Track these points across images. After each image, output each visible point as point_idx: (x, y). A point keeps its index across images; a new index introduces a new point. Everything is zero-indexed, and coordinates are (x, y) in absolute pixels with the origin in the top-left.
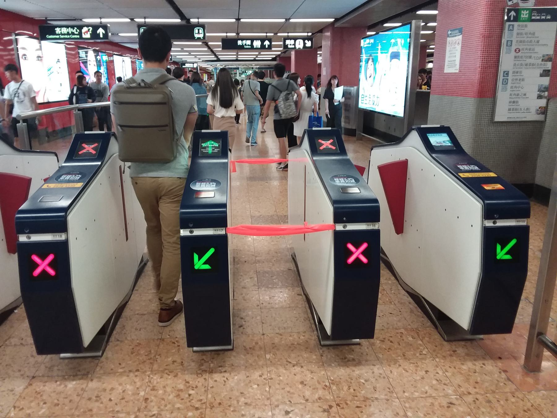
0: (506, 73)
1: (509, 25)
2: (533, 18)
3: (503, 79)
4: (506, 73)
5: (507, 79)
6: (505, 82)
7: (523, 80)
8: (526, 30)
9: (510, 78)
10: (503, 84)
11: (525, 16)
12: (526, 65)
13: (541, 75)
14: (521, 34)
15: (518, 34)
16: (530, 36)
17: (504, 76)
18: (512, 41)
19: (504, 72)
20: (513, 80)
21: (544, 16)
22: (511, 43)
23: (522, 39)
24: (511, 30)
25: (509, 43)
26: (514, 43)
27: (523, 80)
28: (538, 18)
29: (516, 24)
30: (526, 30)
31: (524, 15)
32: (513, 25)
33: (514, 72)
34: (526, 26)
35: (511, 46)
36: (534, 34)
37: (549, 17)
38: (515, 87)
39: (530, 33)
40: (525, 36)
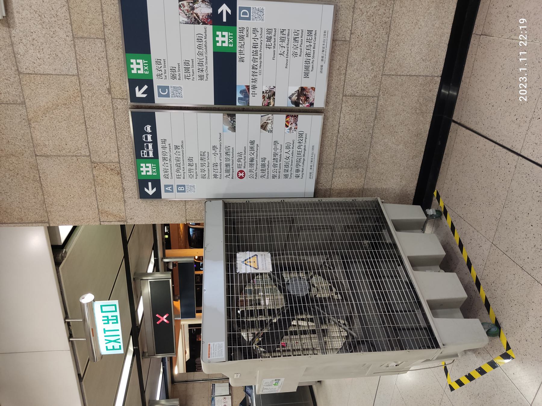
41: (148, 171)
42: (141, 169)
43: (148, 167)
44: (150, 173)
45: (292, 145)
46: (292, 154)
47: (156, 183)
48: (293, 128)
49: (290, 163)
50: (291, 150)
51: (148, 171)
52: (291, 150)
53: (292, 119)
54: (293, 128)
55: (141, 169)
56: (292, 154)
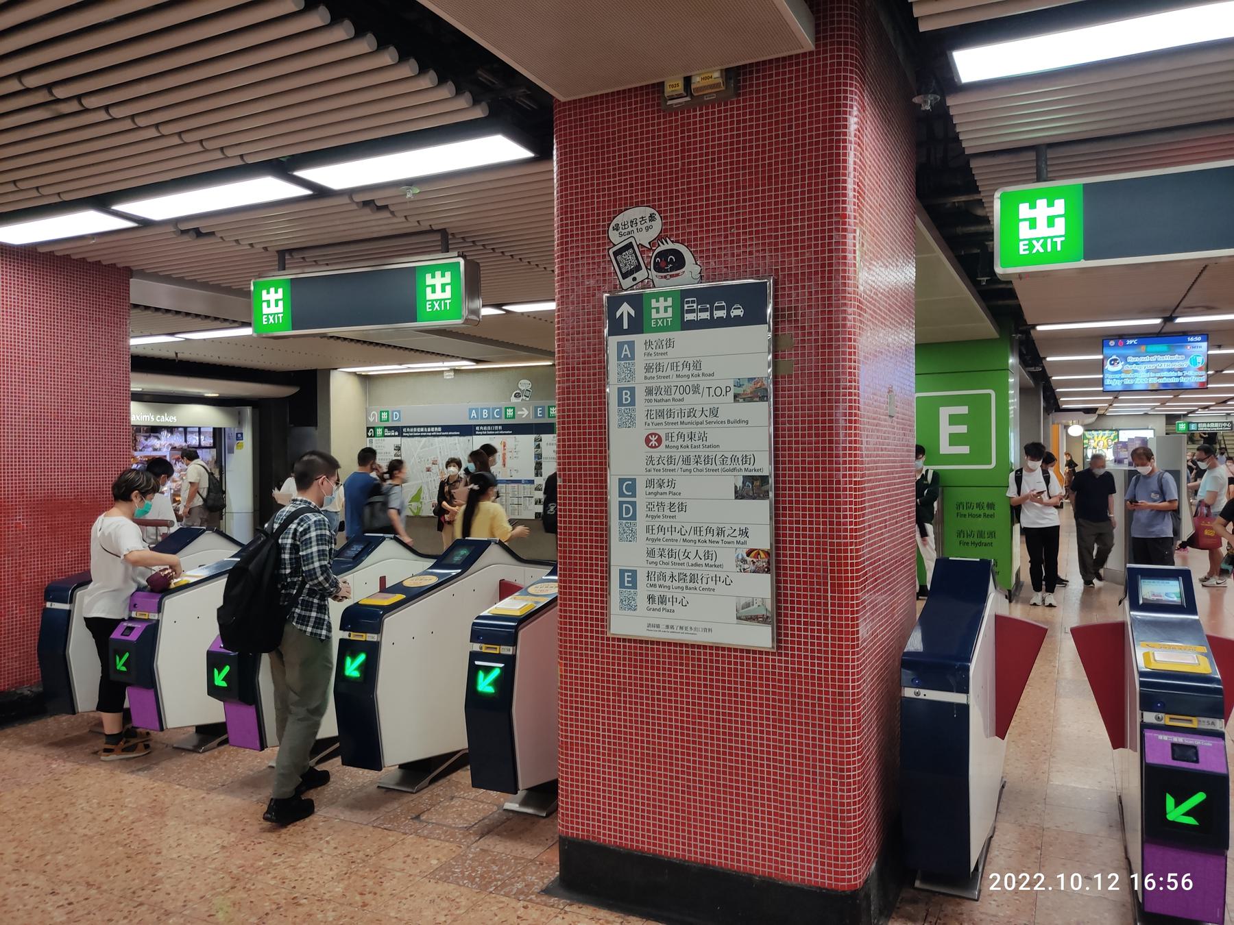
0: (629, 486)
1: (620, 345)
2: (689, 317)
3: (621, 503)
4: (629, 486)
5: (634, 504)
6: (629, 514)
7: (682, 507)
8: (673, 354)
9: (641, 499)
10: (621, 518)
11: (662, 314)
12: (687, 460)
13: (739, 495)
14: (659, 367)
15: (648, 368)
16: (686, 371)
17: (621, 494)
18: (632, 390)
19: (621, 481)
20: (650, 506)
21: (721, 308)
22: (633, 396)
23: (663, 384)
24: (626, 358)
25: (626, 396)
26: (640, 395)
27: (682, 507)
28: (705, 315)
29: (639, 339)
30: (673, 354)
31: (661, 310)
32: (631, 345)
33: (650, 483)
34: (670, 343)
35: (633, 403)
36: (697, 365)
37: (738, 312)
38: (661, 529)
39: (686, 365)
40: (669, 372)
41: (658, 312)
42: (662, 299)
43: (666, 311)
44: (654, 315)
45: (712, 563)
46: (696, 565)
47: (637, 325)
48: (746, 566)
49: (677, 560)
50: (703, 562)
51: (658, 312)
52: (703, 562)
53: (762, 563)
54: (746, 566)
55: (662, 299)
56: (696, 565)
